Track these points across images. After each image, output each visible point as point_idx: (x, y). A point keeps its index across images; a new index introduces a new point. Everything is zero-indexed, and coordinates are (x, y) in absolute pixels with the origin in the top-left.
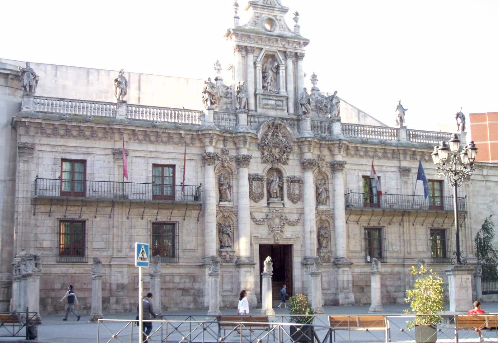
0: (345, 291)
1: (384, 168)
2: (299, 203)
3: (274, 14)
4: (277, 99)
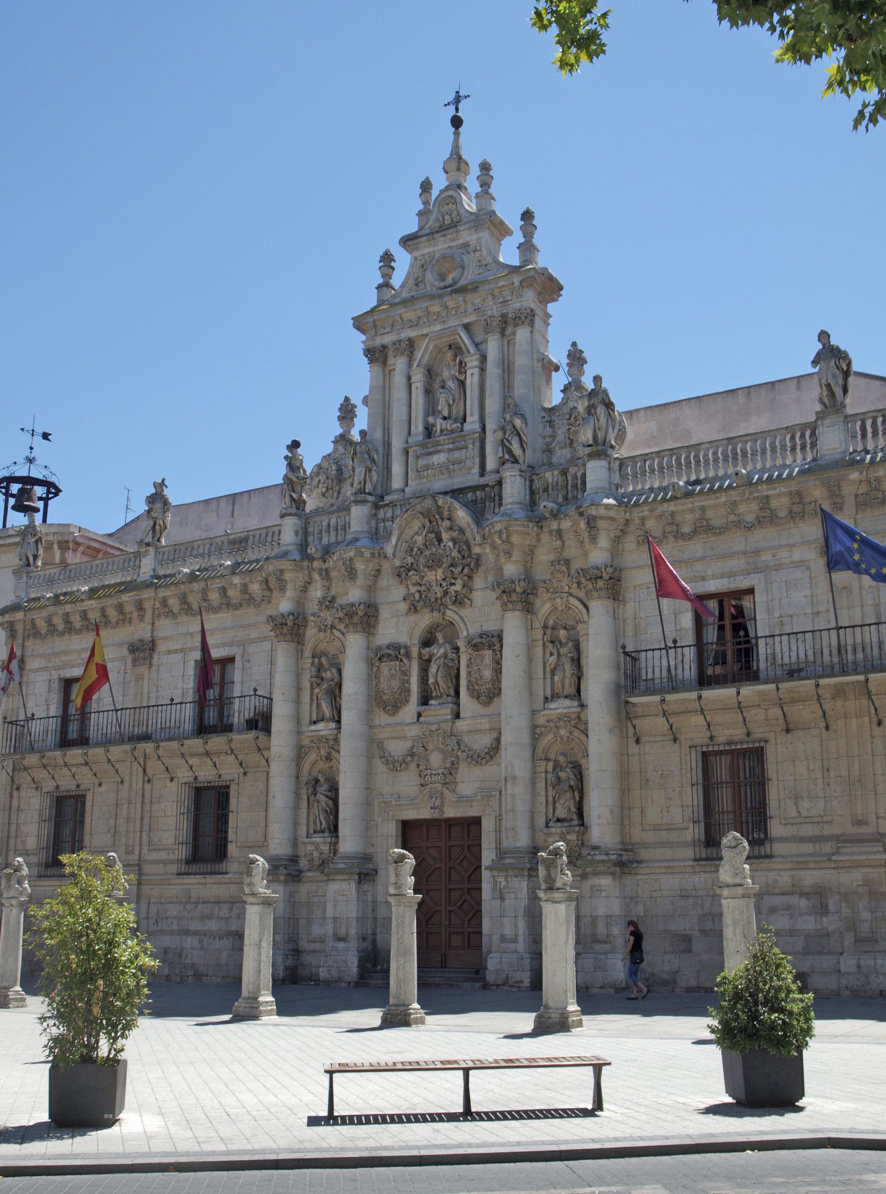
0: (597, 947)
1: (766, 557)
2: (496, 700)
3: (461, 241)
4: (451, 446)
